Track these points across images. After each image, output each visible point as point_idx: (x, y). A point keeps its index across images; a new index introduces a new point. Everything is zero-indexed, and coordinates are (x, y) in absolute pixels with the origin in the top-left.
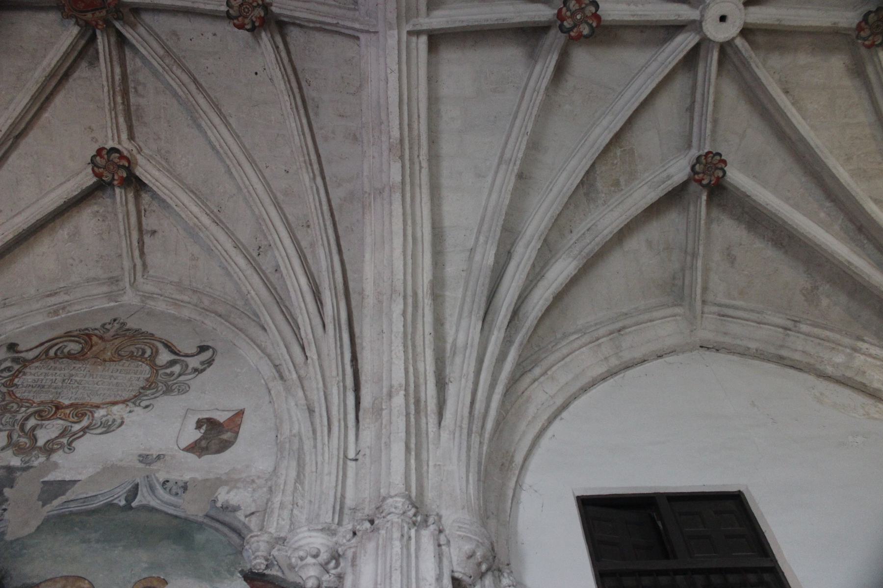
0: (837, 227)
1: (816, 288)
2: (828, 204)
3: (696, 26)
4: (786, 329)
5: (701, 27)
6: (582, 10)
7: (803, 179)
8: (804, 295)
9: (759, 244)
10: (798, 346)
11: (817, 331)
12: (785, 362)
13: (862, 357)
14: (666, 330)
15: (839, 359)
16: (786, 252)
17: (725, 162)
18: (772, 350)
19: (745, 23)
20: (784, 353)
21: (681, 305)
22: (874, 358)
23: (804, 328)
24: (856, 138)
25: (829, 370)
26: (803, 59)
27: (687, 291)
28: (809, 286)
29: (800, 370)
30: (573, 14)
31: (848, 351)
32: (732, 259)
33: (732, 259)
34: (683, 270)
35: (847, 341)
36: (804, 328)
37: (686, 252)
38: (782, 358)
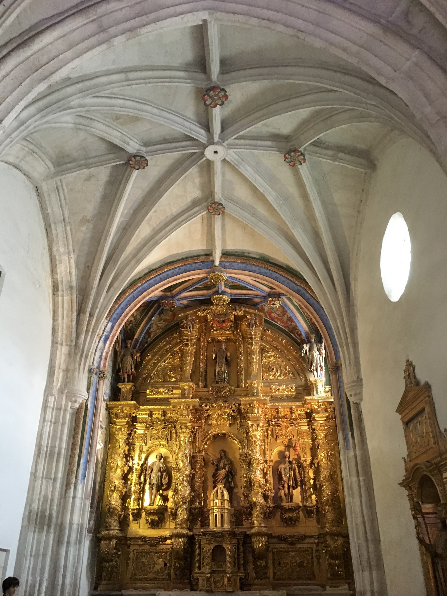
0: (122, 220)
1: (89, 221)
2: (132, 212)
3: (211, 142)
4: (64, 220)
5: (211, 144)
6: (219, 99)
7: (140, 197)
8: (83, 218)
9: (101, 189)
10: (58, 231)
11: (69, 233)
12: (48, 229)
13: (67, 258)
14: (39, 168)
15: (62, 250)
16: (101, 202)
17: (144, 168)
18: (52, 220)
19: (213, 161)
20: (53, 226)
21: (54, 167)
22: (69, 262)
23: (68, 228)
24: (165, 211)
25: (55, 249)
26: (197, 181)
27: (64, 167)
28: (88, 218)
29: (48, 237)
30: (217, 95)
31: (67, 250)
32: (88, 179)
33: (88, 179)
34: (74, 160)
35: (71, 248)
36: (68, 228)
37: (86, 159)
38: (50, 226)
